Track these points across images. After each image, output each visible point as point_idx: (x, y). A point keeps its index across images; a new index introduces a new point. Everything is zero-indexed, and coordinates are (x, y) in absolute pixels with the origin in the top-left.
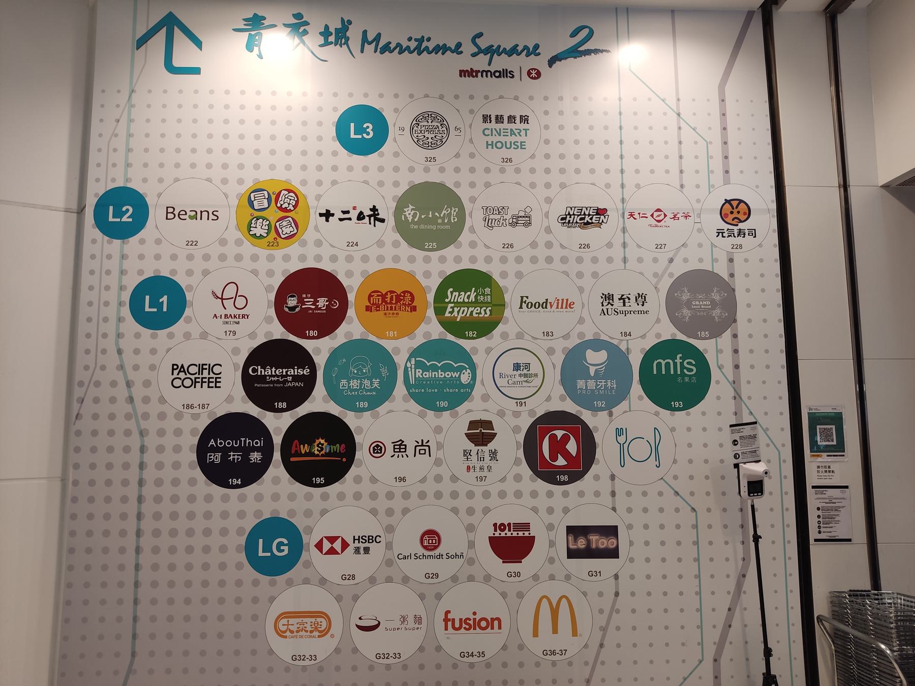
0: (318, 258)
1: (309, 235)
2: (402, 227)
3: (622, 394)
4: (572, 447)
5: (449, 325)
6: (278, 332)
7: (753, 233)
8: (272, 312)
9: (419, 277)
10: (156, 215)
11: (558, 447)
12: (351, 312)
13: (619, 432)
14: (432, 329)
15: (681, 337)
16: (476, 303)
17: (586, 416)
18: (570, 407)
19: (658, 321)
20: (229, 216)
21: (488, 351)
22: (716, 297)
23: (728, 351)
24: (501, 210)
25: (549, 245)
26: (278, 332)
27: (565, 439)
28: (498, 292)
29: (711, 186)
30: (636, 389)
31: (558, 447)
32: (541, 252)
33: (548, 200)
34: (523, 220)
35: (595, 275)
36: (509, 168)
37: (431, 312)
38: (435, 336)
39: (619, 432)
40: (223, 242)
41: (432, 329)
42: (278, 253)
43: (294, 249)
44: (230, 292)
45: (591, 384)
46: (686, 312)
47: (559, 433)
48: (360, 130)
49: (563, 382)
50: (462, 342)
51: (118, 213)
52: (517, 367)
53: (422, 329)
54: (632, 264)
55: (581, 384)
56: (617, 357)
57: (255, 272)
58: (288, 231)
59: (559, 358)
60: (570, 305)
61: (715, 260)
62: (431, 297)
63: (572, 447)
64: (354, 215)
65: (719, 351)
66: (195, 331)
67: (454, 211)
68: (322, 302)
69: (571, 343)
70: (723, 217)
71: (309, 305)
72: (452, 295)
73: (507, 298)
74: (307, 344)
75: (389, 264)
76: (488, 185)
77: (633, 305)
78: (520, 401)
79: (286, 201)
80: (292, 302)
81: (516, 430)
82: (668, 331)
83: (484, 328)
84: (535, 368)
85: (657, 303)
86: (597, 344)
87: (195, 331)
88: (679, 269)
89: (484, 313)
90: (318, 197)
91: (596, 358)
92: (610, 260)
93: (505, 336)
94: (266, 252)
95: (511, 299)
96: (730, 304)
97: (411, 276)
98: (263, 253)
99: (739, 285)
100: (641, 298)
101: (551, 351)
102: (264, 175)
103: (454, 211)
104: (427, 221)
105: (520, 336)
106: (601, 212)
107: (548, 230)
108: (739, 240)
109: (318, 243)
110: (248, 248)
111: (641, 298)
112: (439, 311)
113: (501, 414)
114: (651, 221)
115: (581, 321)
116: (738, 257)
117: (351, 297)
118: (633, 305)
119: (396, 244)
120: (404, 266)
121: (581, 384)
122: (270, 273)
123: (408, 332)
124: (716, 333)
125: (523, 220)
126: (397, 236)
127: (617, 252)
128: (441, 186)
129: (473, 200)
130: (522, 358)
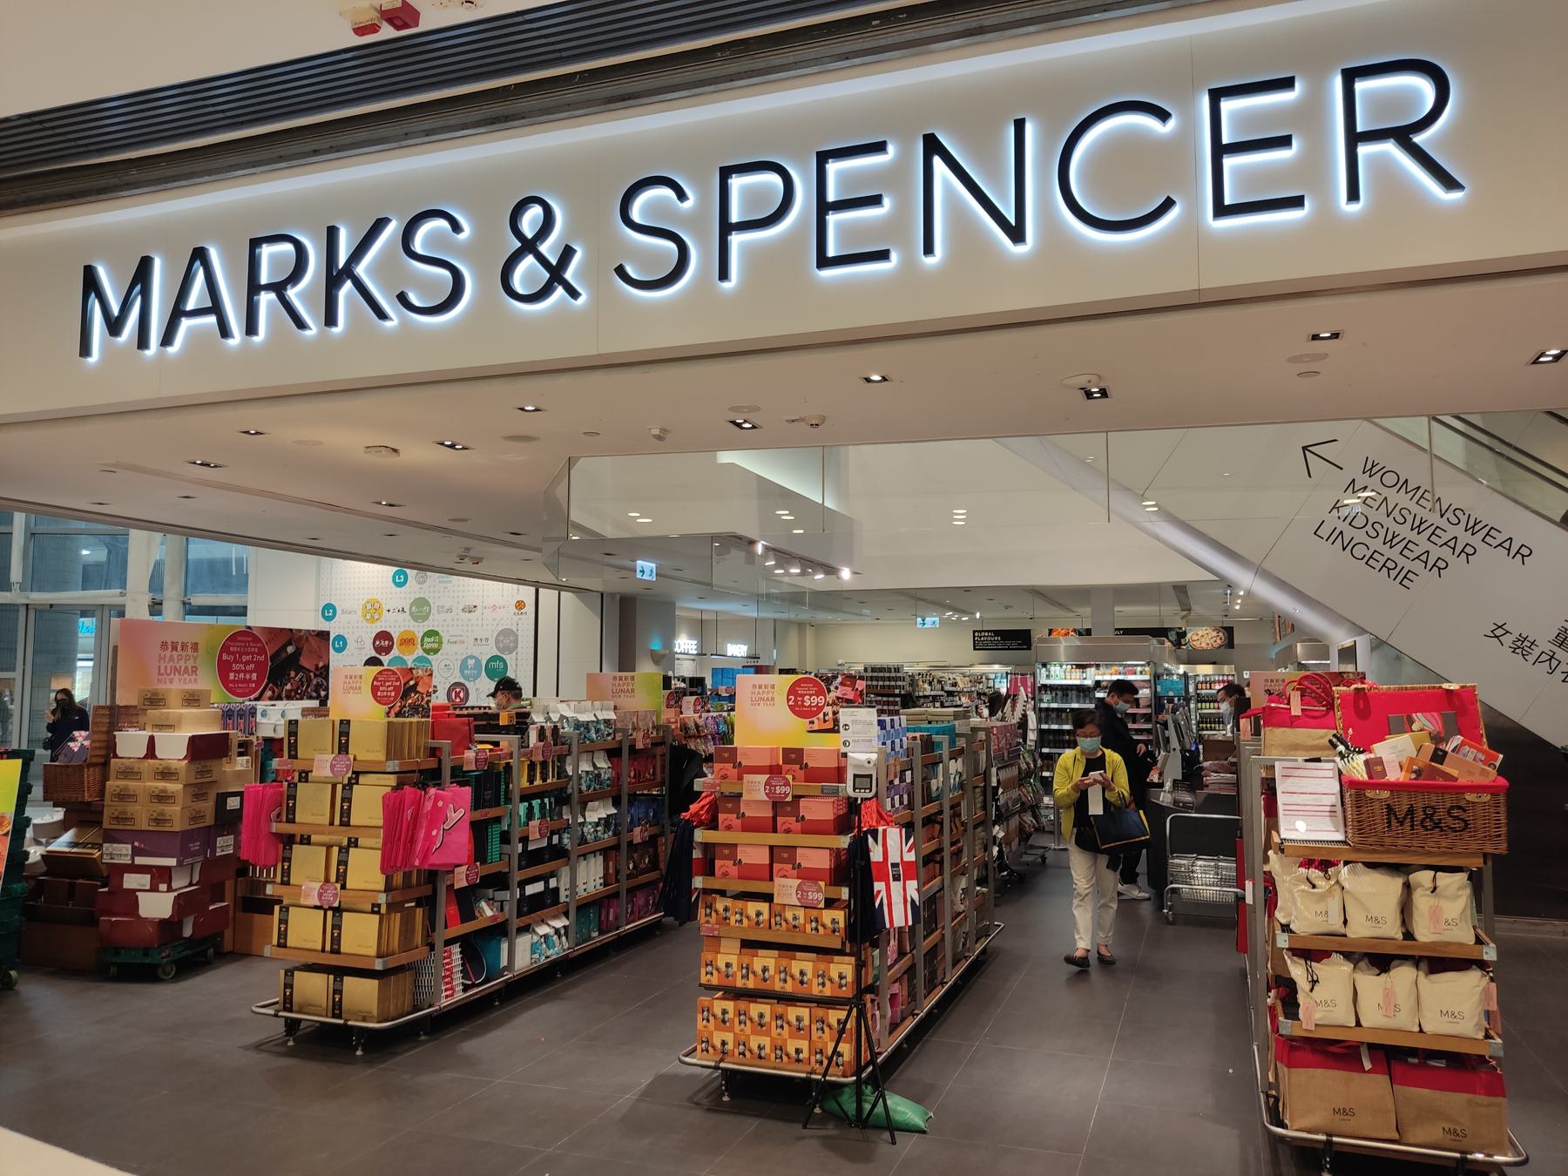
0: (386, 627)
1: (383, 618)
2: (411, 614)
3: (479, 675)
4: (462, 695)
5: (427, 651)
6: (374, 654)
7: (526, 613)
8: (372, 647)
9: (416, 633)
10: (339, 612)
11: (457, 695)
12: (395, 646)
13: (477, 689)
14: (419, 652)
15: (499, 654)
16: (434, 642)
17: (467, 684)
18: (462, 680)
19: (492, 648)
20: (360, 613)
21: (437, 660)
22: (512, 639)
23: (514, 658)
24: (443, 607)
25: (458, 620)
26: (374, 654)
27: (460, 692)
28: (441, 638)
29: (513, 596)
30: (483, 673)
31: (457, 695)
32: (455, 622)
33: (458, 603)
34: (450, 610)
35: (472, 631)
36: (446, 590)
37: (419, 646)
38: (420, 655)
39: (477, 689)
40: (358, 622)
41: (419, 652)
42: (374, 625)
43: (378, 624)
44: (359, 640)
45: (469, 672)
46: (501, 645)
47: (458, 690)
48: (400, 578)
49: (460, 671)
50: (428, 657)
51: (328, 613)
52: (446, 666)
53: (416, 652)
54: (485, 627)
55: (466, 672)
56: (478, 661)
57: (367, 632)
58: (376, 617)
59: (459, 663)
60: (464, 642)
61: (512, 625)
62: (419, 640)
63: (462, 695)
64: (397, 610)
65: (511, 659)
66: (350, 654)
67: (428, 608)
68: (387, 642)
69: (465, 656)
70: (516, 607)
71: (383, 644)
72: (426, 639)
73: (443, 640)
74: (381, 658)
75: (407, 628)
76: (439, 597)
77: (484, 642)
78: (446, 678)
79: (377, 606)
80: (378, 643)
81: (445, 688)
82: (495, 652)
83: (436, 651)
84: (451, 666)
85: (492, 641)
86: (472, 657)
87: (350, 654)
88: (500, 628)
89: (436, 646)
90: (386, 604)
91: (471, 662)
92: (477, 625)
93: (442, 654)
94: (371, 625)
95: (445, 640)
96: (516, 641)
97: (413, 632)
98: (369, 625)
99: (519, 634)
100: (487, 639)
101: (457, 660)
102: (370, 597)
103: (428, 608)
104: (419, 612)
105: (447, 654)
106: (475, 607)
107: (458, 614)
108: (521, 616)
109: (386, 621)
110: (365, 623)
111: (487, 639)
112: (422, 645)
113: (440, 683)
114: (491, 609)
115: (467, 648)
116: (520, 622)
117: (395, 641)
118: (484, 642)
119: (409, 621)
120: (411, 629)
121: (466, 672)
122: (371, 632)
123: (412, 653)
124: (511, 653)
125: (450, 610)
126: (410, 618)
127: (480, 622)
128: (424, 598)
129: (434, 603)
130: (447, 662)
